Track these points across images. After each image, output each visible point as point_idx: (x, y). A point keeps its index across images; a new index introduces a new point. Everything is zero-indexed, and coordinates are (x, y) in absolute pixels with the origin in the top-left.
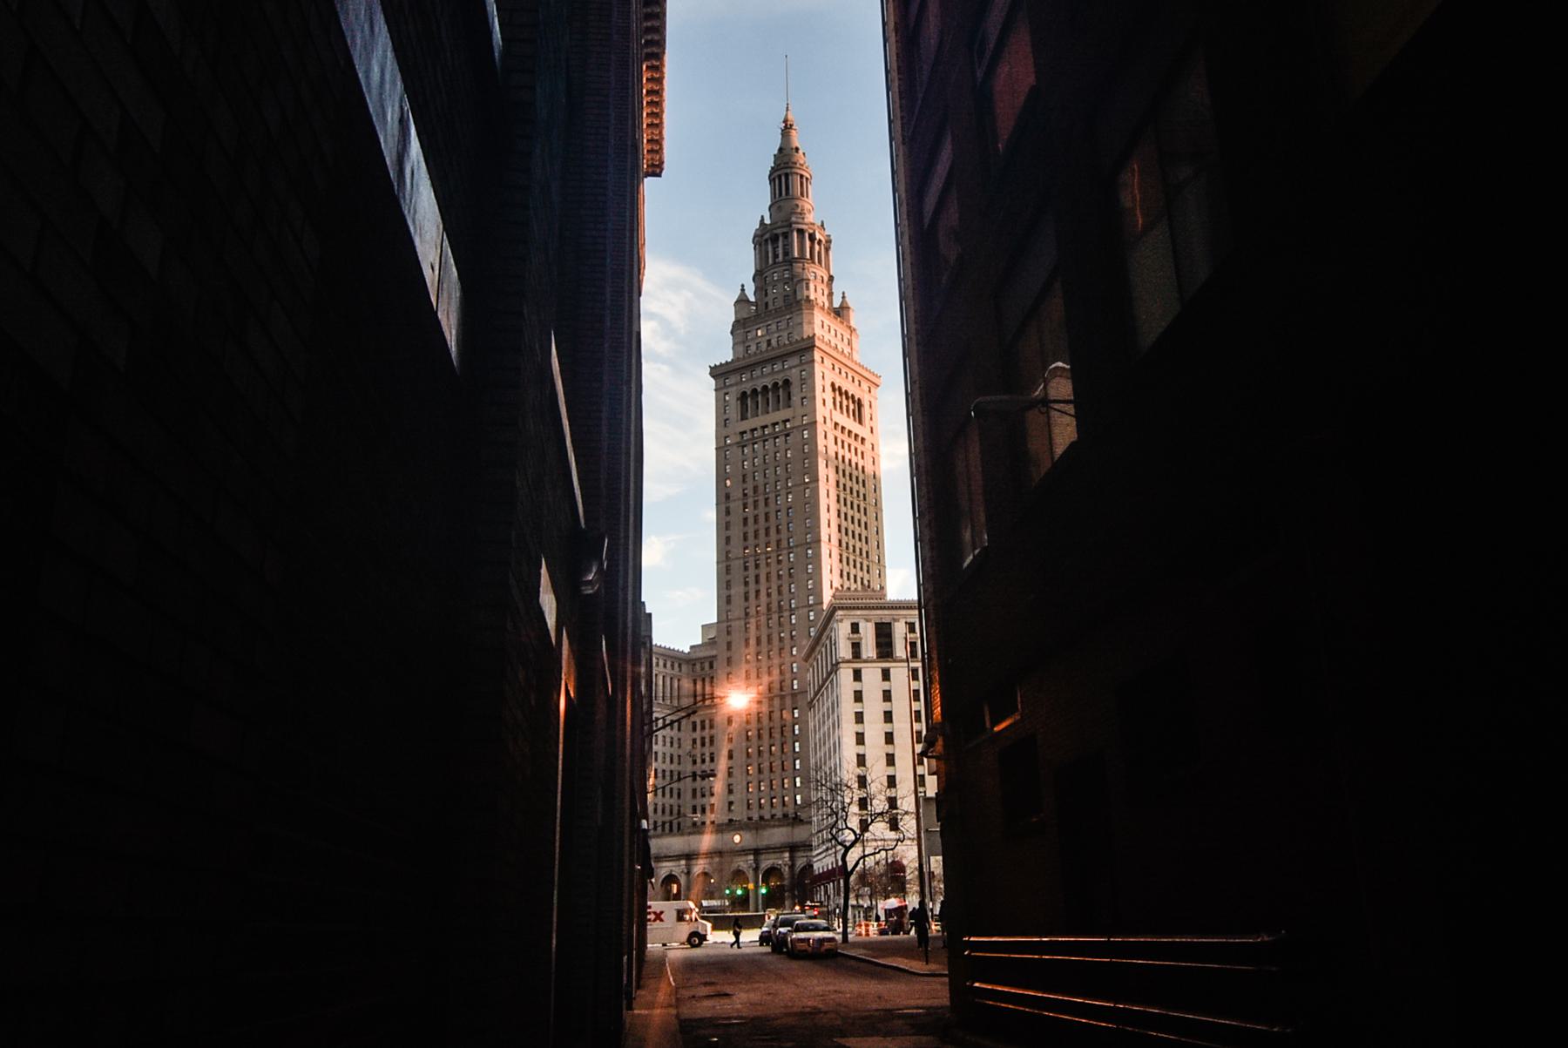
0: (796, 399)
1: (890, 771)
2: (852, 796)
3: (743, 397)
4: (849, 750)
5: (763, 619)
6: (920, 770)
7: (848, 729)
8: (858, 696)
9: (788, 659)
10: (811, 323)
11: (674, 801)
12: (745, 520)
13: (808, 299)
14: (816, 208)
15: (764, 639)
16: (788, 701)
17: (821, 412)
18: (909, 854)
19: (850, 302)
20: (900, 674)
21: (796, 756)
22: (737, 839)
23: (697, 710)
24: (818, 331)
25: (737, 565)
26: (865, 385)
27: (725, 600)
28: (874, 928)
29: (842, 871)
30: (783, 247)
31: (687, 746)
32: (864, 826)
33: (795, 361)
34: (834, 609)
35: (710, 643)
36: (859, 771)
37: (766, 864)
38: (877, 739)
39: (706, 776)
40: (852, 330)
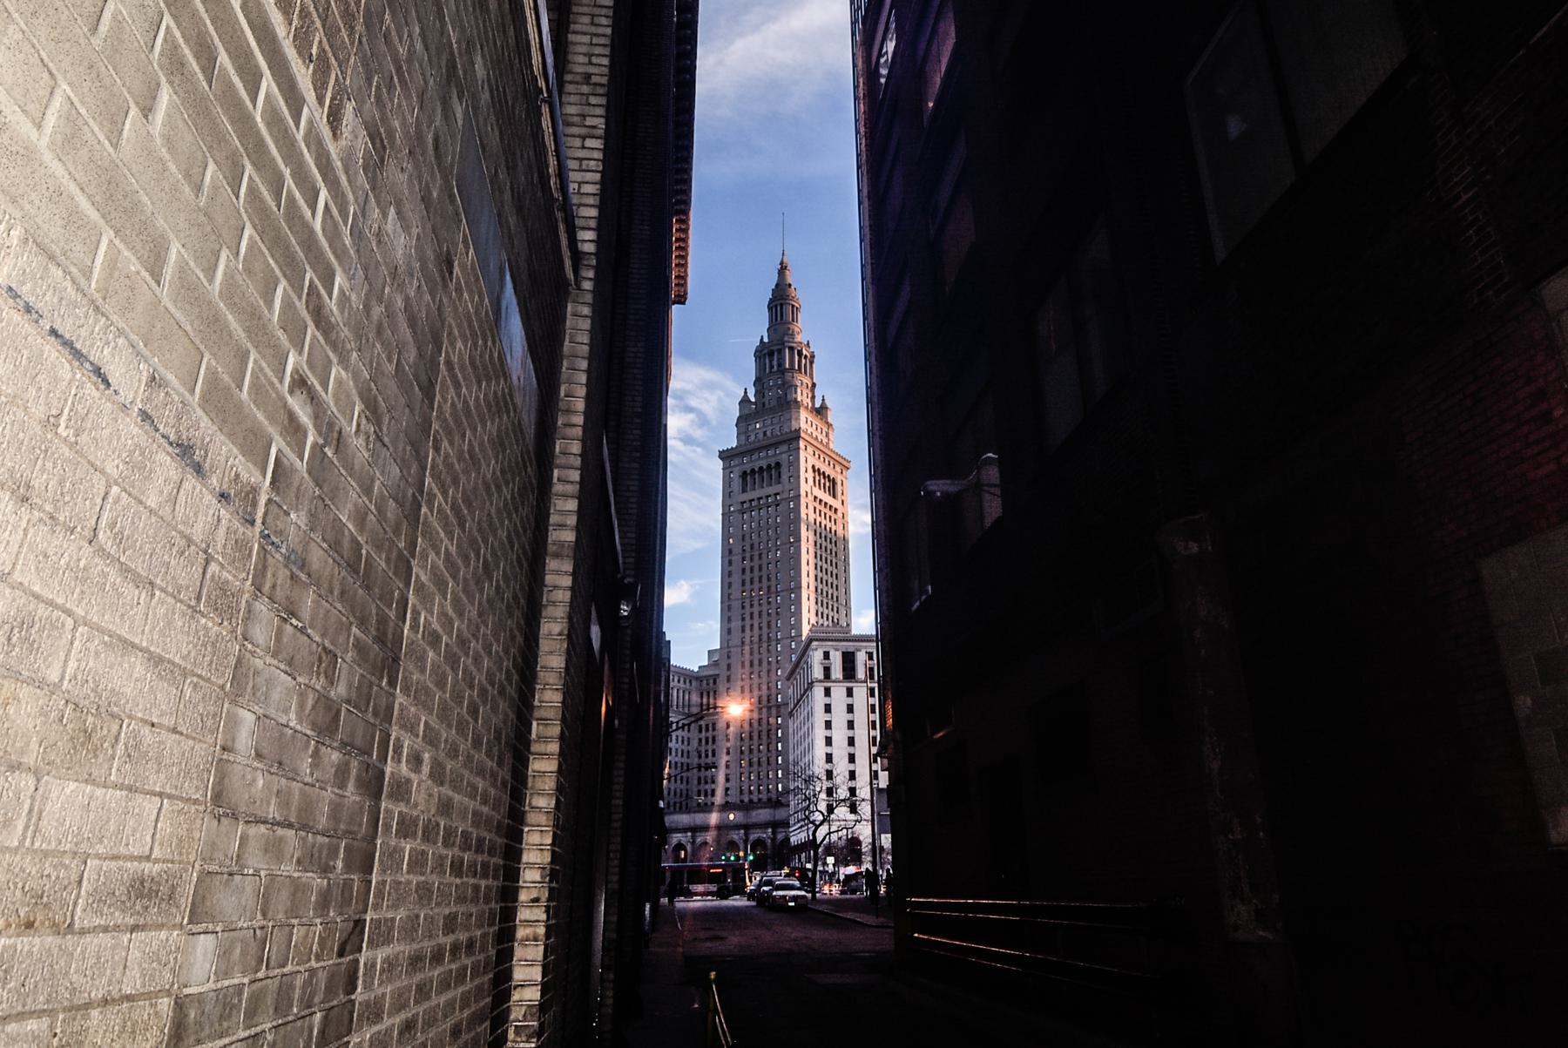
0: (784, 477)
1: (852, 767)
2: (821, 786)
4: (820, 750)
5: (756, 647)
6: (874, 767)
7: (820, 733)
8: (828, 709)
9: (774, 678)
10: (798, 419)
11: (683, 787)
12: (744, 570)
13: (796, 400)
14: (805, 330)
15: (756, 662)
16: (774, 711)
17: (804, 488)
18: (864, 832)
20: (860, 692)
21: (779, 753)
22: (732, 817)
23: (704, 717)
24: (803, 426)
25: (736, 605)
26: (838, 468)
27: (727, 632)
28: (836, 889)
29: (812, 844)
30: (778, 361)
31: (695, 743)
32: (831, 809)
33: (784, 448)
34: (810, 640)
35: (715, 664)
36: (828, 767)
37: (753, 837)
38: (841, 743)
39: (708, 767)
40: (829, 425)
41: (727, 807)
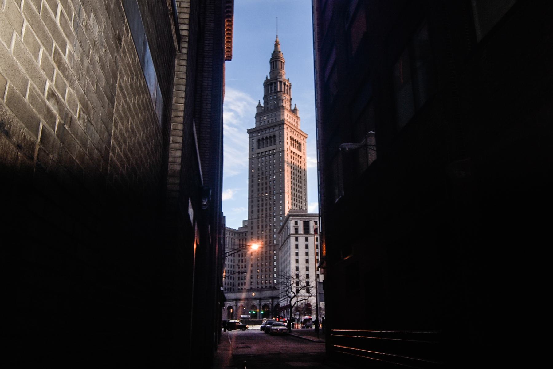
0: (277, 142)
1: (307, 273)
2: (293, 281)
3: (259, 141)
4: (293, 265)
5: (264, 219)
6: (318, 273)
7: (293, 258)
8: (297, 247)
9: (272, 233)
10: (283, 115)
11: (232, 281)
12: (259, 184)
13: (283, 107)
14: (287, 73)
15: (264, 226)
16: (272, 248)
17: (286, 147)
18: (313, 301)
19: (298, 108)
20: (312, 239)
21: (275, 266)
22: (253, 294)
23: (241, 250)
24: (286, 118)
25: (255, 200)
26: (302, 138)
27: (251, 212)
28: (300, 326)
29: (290, 306)
30: (274, 87)
31: (237, 262)
32: (298, 291)
33: (277, 128)
34: (289, 216)
35: (245, 227)
36: (296, 272)
37: (263, 303)
38: (303, 260)
39: (243, 273)
40: (298, 118)
41: (251, 290)
